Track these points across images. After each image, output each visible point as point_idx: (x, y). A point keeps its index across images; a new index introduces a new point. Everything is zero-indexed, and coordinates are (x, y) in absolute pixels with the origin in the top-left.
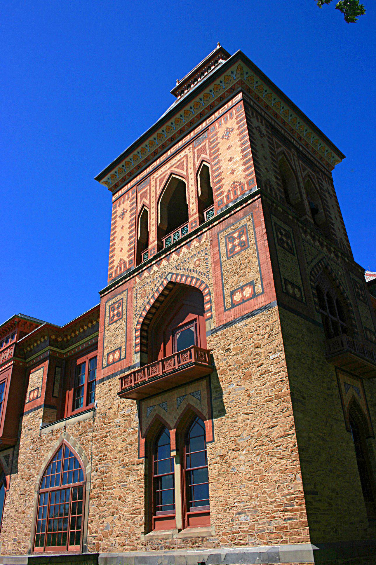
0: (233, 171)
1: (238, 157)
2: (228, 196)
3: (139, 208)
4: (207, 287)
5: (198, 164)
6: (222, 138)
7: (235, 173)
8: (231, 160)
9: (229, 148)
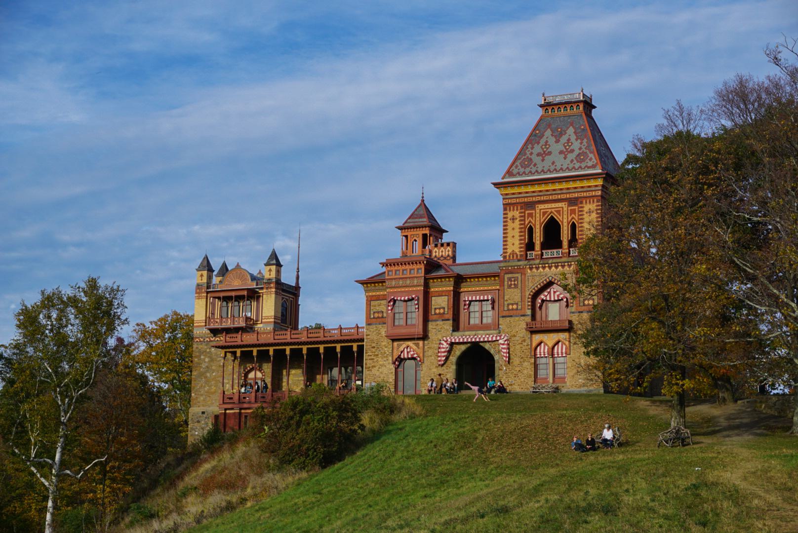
3: (527, 223)
5: (570, 218)
6: (587, 213)
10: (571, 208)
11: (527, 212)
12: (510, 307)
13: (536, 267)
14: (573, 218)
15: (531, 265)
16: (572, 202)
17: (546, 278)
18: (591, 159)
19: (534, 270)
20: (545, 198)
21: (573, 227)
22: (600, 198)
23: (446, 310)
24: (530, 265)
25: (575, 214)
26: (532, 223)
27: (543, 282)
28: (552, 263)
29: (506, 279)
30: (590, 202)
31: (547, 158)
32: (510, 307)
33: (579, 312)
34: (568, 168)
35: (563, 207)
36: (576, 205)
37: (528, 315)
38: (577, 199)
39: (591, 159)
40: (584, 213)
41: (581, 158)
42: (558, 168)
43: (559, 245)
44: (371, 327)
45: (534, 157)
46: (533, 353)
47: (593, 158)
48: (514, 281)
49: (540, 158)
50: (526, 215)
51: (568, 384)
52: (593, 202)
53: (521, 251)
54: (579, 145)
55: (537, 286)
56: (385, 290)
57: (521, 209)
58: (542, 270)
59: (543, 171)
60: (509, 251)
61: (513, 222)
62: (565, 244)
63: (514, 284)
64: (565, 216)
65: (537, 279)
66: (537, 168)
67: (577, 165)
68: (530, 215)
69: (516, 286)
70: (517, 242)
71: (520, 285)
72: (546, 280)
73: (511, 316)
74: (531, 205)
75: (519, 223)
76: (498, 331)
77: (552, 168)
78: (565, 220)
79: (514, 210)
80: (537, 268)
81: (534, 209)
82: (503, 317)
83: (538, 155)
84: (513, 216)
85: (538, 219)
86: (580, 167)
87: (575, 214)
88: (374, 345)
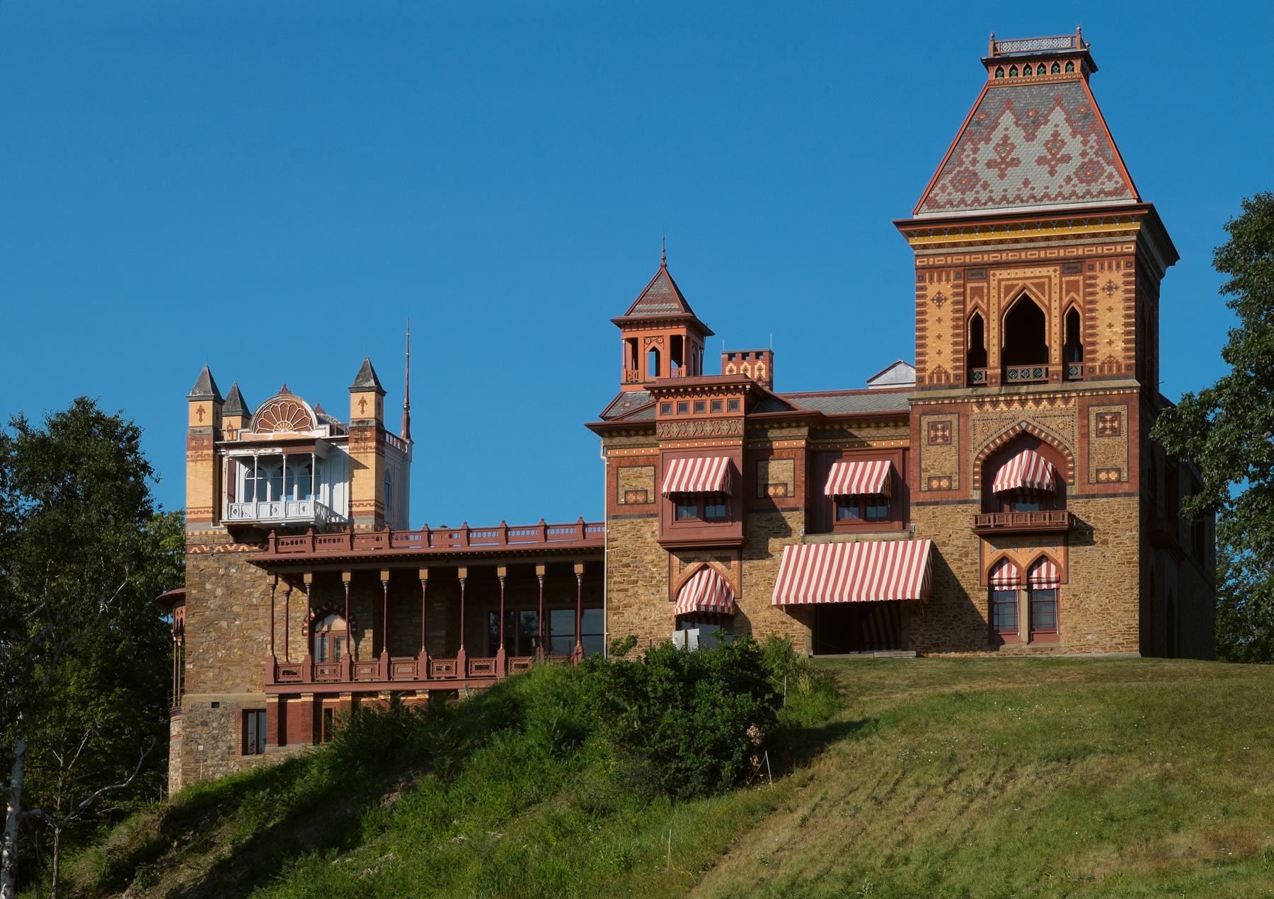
0: (1110, 343)
1: (1119, 329)
2: (1101, 368)
3: (969, 308)
4: (1070, 454)
5: (1066, 300)
6: (1103, 289)
7: (1113, 345)
8: (1110, 326)
9: (1110, 309)
10: (1067, 279)
11: (969, 285)
12: (935, 484)
13: (992, 401)
14: (1072, 301)
15: (982, 396)
16: (1070, 266)
17: (1014, 424)
18: (1110, 177)
19: (988, 407)
20: (1010, 257)
21: (1072, 320)
22: (1132, 259)
23: (791, 488)
24: (977, 396)
25: (1077, 291)
26: (982, 309)
27: (1007, 433)
28: (1027, 394)
29: (925, 426)
30: (1110, 267)
31: (1010, 171)
32: (935, 484)
33: (1088, 496)
34: (1060, 194)
35: (1049, 277)
36: (1080, 272)
37: (974, 502)
38: (1081, 259)
40: (1098, 289)
41: (1088, 172)
42: (1039, 193)
43: (1041, 355)
44: (620, 522)
45: (980, 169)
46: (985, 581)
47: (1115, 173)
48: (943, 430)
49: (996, 171)
50: (968, 292)
51: (1062, 643)
52: (1118, 266)
53: (956, 368)
54: (1080, 148)
55: (994, 442)
56: (656, 445)
57: (956, 278)
58: (1005, 408)
59: (1004, 198)
60: (931, 367)
61: (939, 306)
62: (1055, 353)
63: (943, 437)
64: (1055, 296)
65: (994, 426)
66: (991, 191)
67: (1081, 188)
68: (977, 292)
69: (947, 441)
70: (948, 349)
71: (955, 438)
72: (1013, 429)
73: (937, 503)
74: (980, 271)
75: (951, 308)
76: (907, 534)
77: (1025, 193)
78: (1055, 305)
79: (940, 280)
80: (995, 404)
81: (986, 279)
82: (918, 504)
83: (990, 165)
84: (939, 293)
85: (994, 301)
86: (1088, 193)
87: (1077, 291)
88: (625, 560)
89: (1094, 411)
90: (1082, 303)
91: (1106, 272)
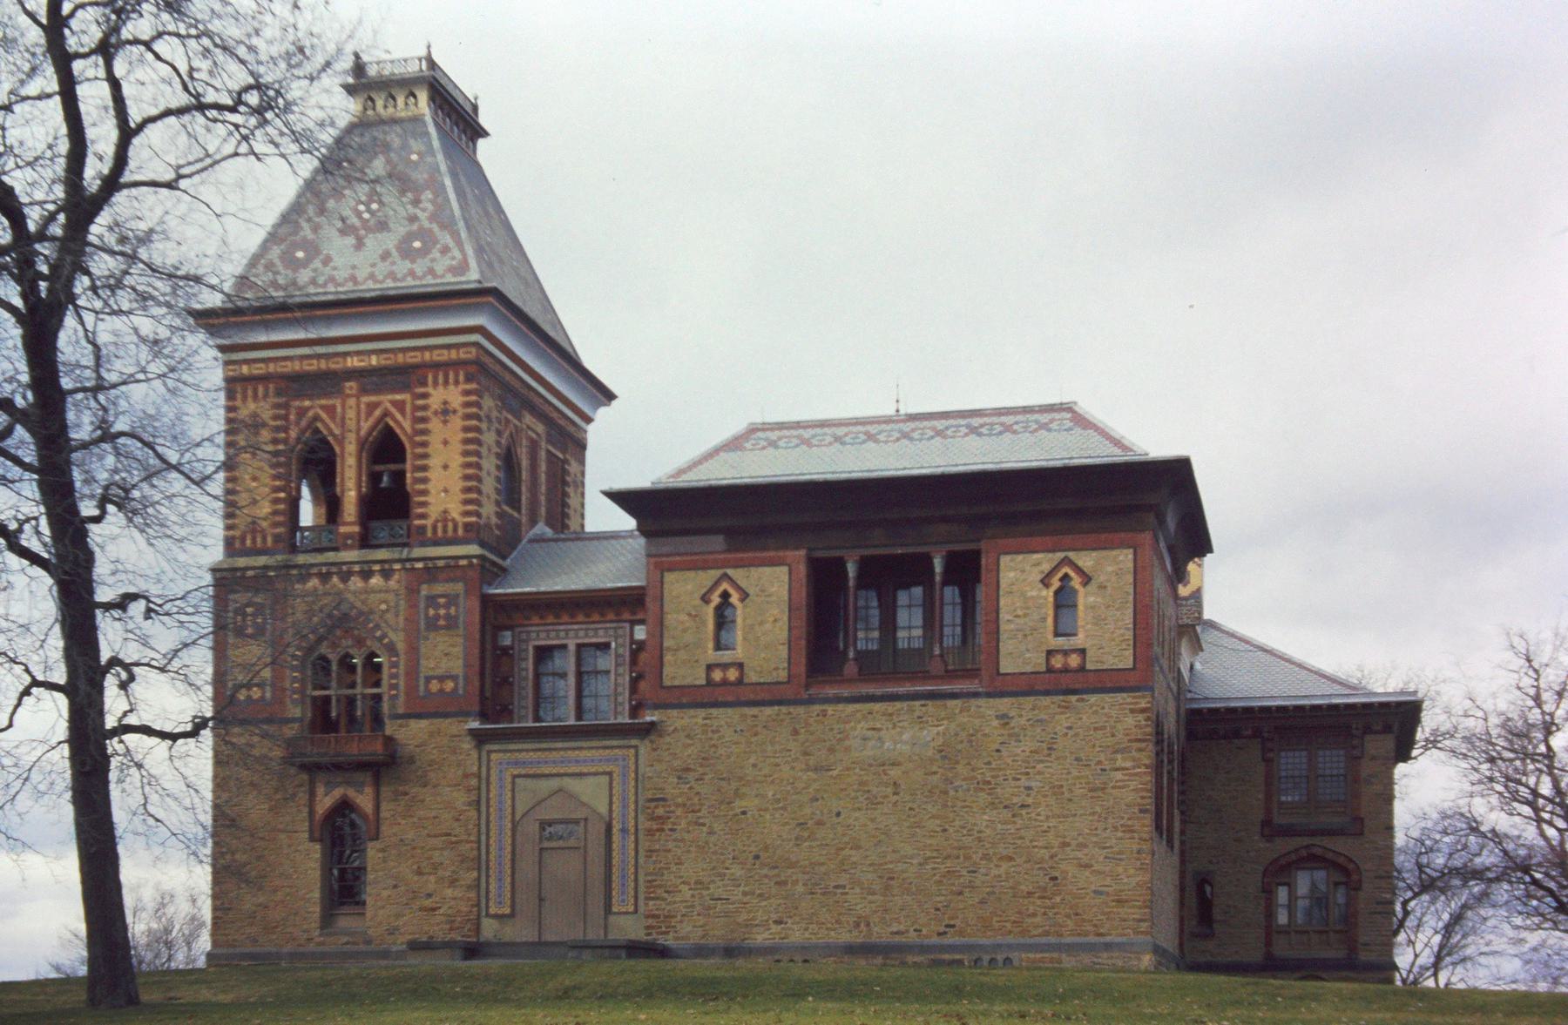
39: (445, 250)
89: (425, 590)
90: (409, 430)
91: (441, 388)
